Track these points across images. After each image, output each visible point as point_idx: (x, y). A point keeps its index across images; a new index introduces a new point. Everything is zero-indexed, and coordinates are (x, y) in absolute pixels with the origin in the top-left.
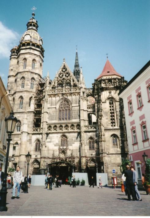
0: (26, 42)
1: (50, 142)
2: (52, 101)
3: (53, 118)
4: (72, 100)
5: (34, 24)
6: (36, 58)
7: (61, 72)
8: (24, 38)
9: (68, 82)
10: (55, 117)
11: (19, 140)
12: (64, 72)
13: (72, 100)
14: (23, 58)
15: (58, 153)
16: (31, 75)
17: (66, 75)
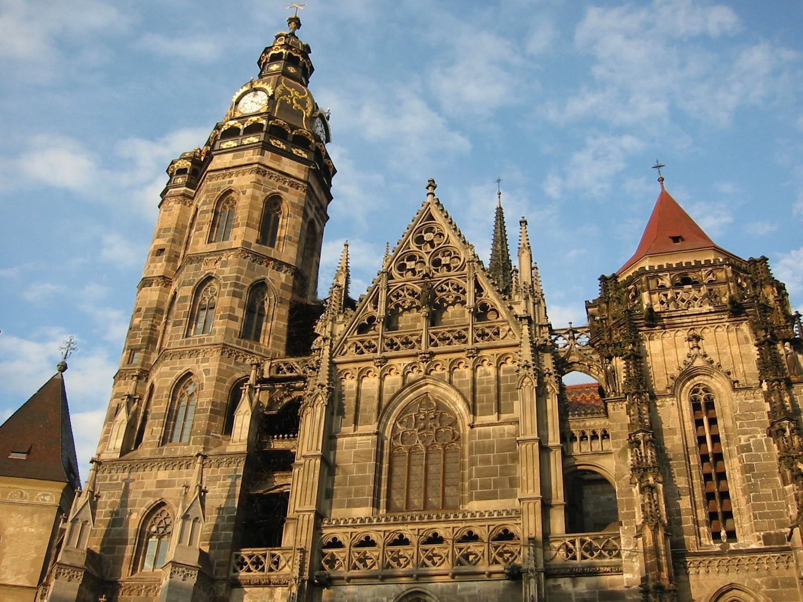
3: (357, 493)
4: (474, 389)
5: (289, 53)
6: (286, 190)
13: (474, 389)
14: (219, 189)
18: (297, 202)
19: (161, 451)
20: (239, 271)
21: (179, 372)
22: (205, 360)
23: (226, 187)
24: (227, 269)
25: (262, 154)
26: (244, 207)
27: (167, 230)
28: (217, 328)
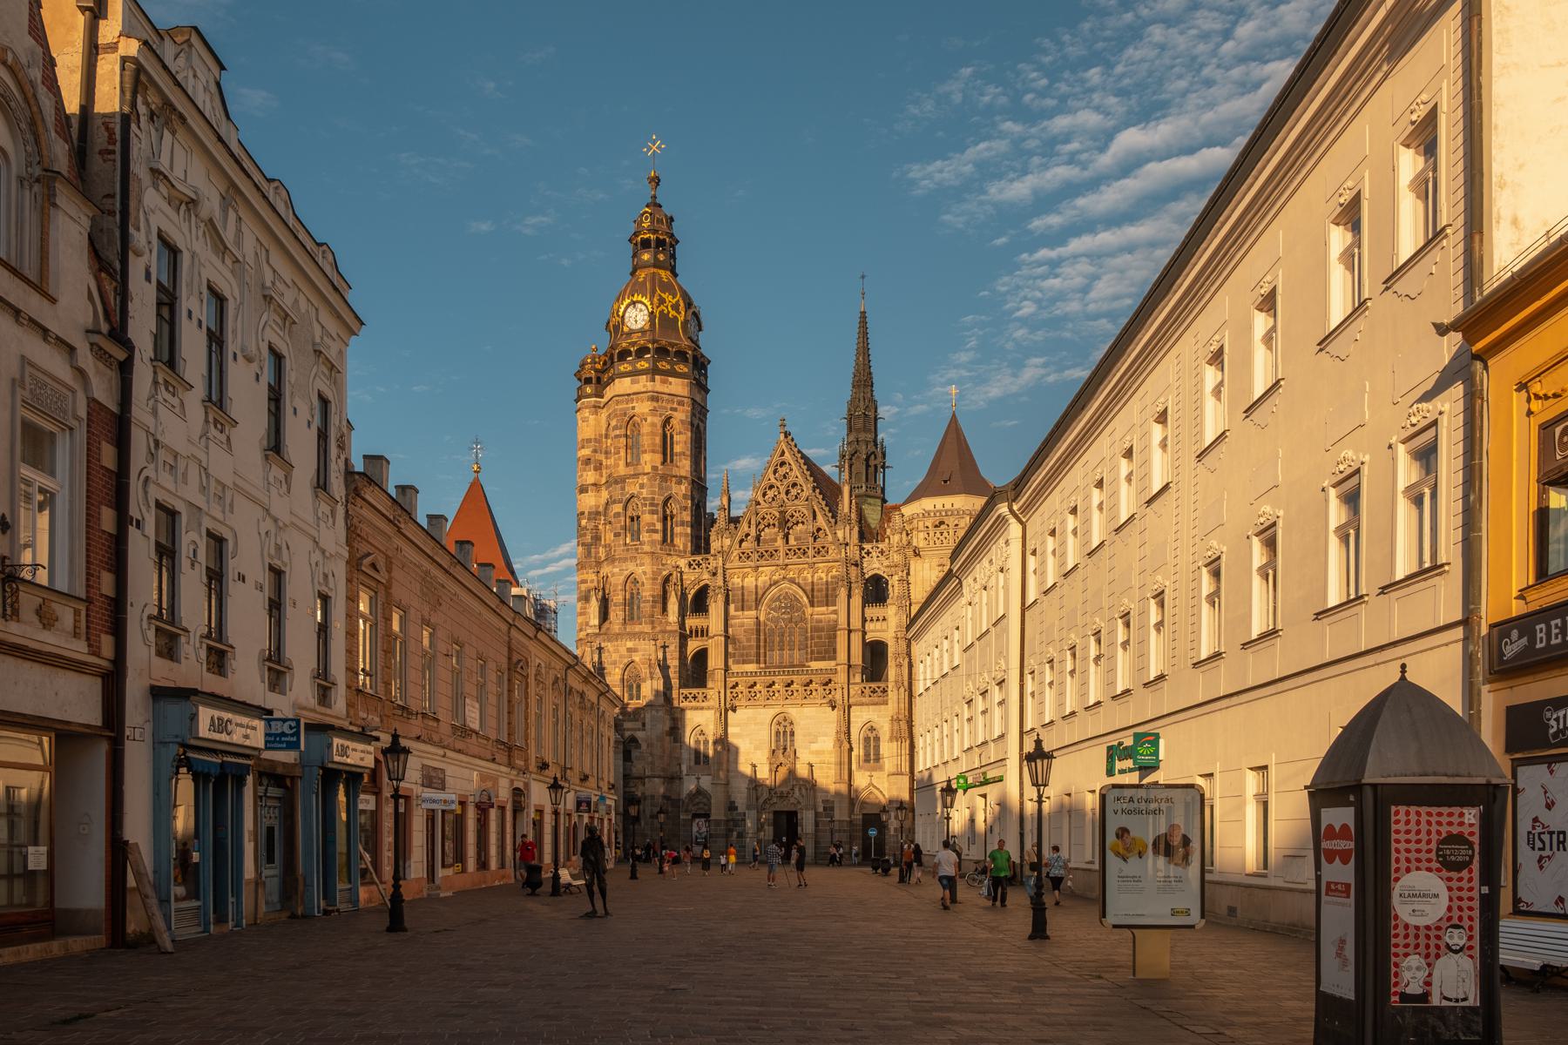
0: (633, 344)
2: (743, 594)
4: (813, 590)
6: (675, 410)
7: (772, 477)
8: (623, 317)
10: (754, 651)
11: (639, 730)
13: (813, 590)
14: (625, 414)
16: (661, 488)
18: (684, 418)
19: (625, 629)
20: (653, 493)
21: (626, 573)
22: (642, 565)
23: (631, 413)
24: (644, 491)
25: (653, 380)
26: (648, 434)
28: (646, 539)
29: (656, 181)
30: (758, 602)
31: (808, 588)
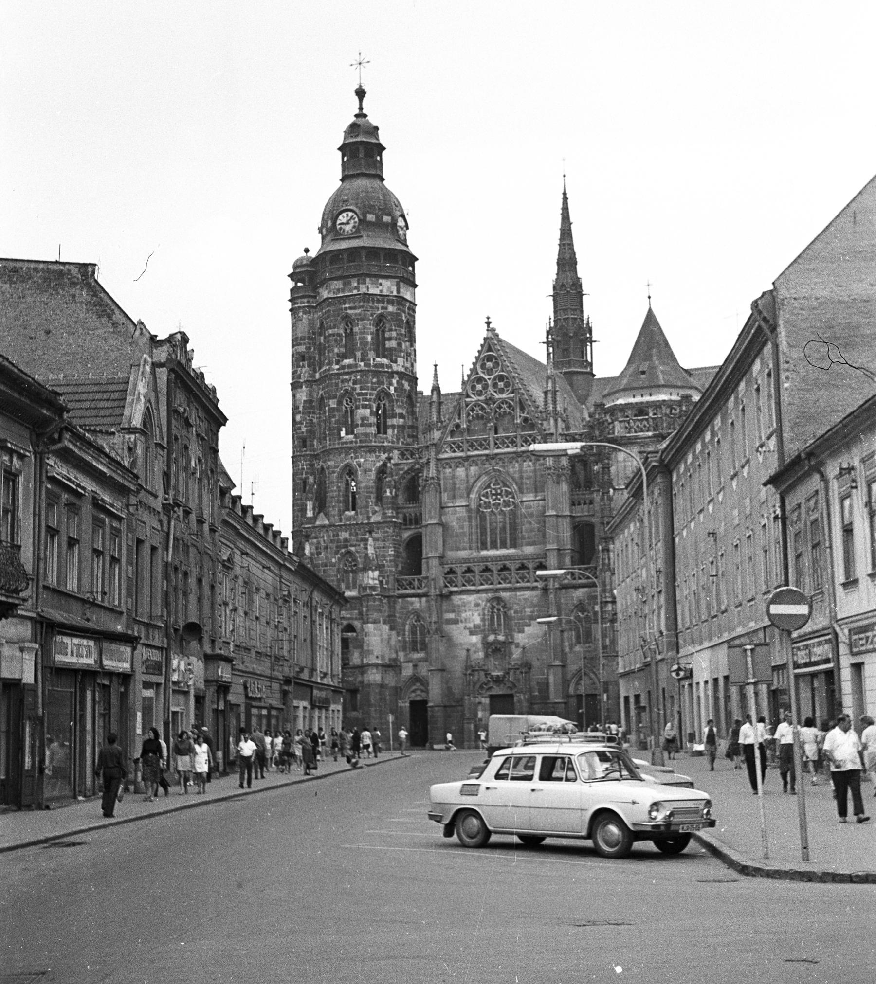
1: (456, 622)
2: (455, 484)
4: (521, 477)
7: (479, 370)
9: (505, 412)
12: (490, 372)
13: (521, 477)
15: (481, 655)
17: (495, 385)
27: (303, 339)
29: (361, 93)
30: (469, 491)
31: (517, 476)
